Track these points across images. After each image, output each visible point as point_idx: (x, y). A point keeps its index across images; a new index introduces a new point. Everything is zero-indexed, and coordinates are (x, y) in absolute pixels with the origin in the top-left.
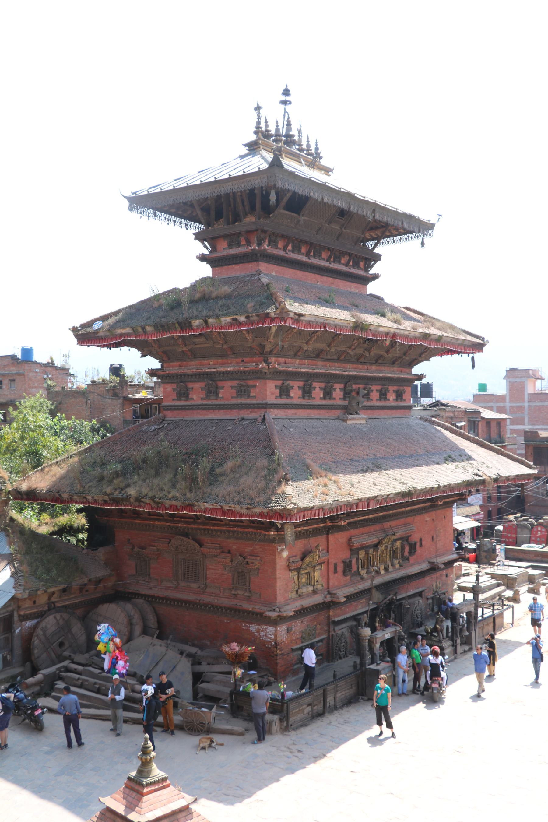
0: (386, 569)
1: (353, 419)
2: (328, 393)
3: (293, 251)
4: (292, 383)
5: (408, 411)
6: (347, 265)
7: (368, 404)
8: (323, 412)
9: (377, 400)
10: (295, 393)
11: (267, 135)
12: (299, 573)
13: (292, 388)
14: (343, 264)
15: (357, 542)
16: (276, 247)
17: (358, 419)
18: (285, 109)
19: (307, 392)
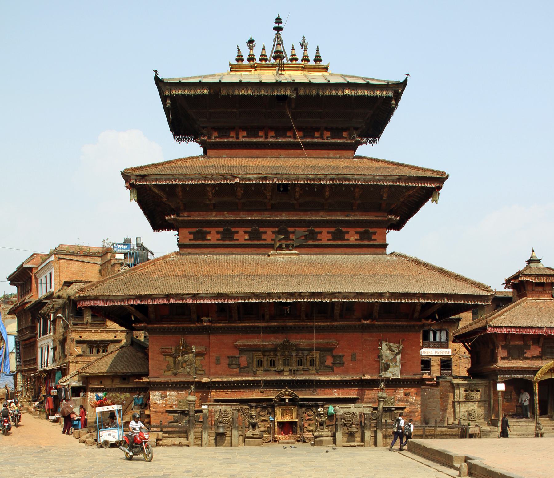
0: (292, 372)
1: (277, 254)
2: (255, 235)
3: (248, 137)
4: (208, 230)
5: (383, 249)
6: (322, 137)
7: (314, 243)
8: (247, 250)
9: (329, 240)
10: (213, 237)
11: (251, 59)
12: (173, 358)
13: (209, 233)
14: (317, 138)
15: (239, 343)
16: (229, 137)
17: (284, 254)
18: (278, 34)
19: (227, 234)
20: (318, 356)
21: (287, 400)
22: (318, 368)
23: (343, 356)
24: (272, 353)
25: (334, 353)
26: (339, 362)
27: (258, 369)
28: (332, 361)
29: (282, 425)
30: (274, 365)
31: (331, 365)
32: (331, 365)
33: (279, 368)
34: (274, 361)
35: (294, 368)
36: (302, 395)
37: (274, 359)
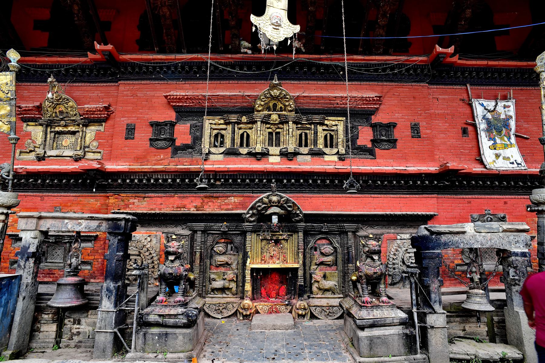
20: (341, 128)
21: (275, 219)
22: (342, 151)
23: (394, 125)
24: (244, 119)
25: (375, 119)
26: (385, 137)
27: (213, 150)
28: (372, 138)
29: (261, 275)
30: (248, 145)
31: (369, 145)
32: (369, 145)
33: (259, 148)
34: (248, 136)
35: (291, 148)
36: (311, 204)
37: (249, 131)
